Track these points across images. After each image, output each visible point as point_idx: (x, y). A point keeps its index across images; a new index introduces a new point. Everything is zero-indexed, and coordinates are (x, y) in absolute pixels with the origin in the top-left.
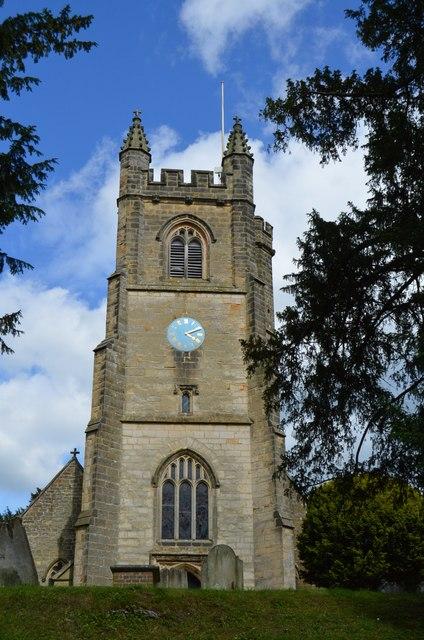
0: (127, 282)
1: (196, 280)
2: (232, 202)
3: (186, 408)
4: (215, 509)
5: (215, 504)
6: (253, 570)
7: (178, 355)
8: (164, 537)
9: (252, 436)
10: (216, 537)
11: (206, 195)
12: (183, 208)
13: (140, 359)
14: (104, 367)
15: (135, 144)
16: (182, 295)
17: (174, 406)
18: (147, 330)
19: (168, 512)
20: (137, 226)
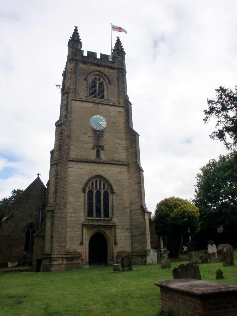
0: (71, 95)
1: (103, 100)
2: (118, 68)
3: (98, 156)
4: (113, 203)
5: (112, 201)
6: (129, 231)
7: (95, 131)
8: (89, 216)
9: (128, 171)
10: (113, 215)
11: (106, 64)
12: (97, 68)
13: (77, 132)
14: (61, 133)
15: (75, 39)
16: (96, 105)
17: (93, 155)
18: (80, 119)
19: (90, 204)
20: (76, 73)
